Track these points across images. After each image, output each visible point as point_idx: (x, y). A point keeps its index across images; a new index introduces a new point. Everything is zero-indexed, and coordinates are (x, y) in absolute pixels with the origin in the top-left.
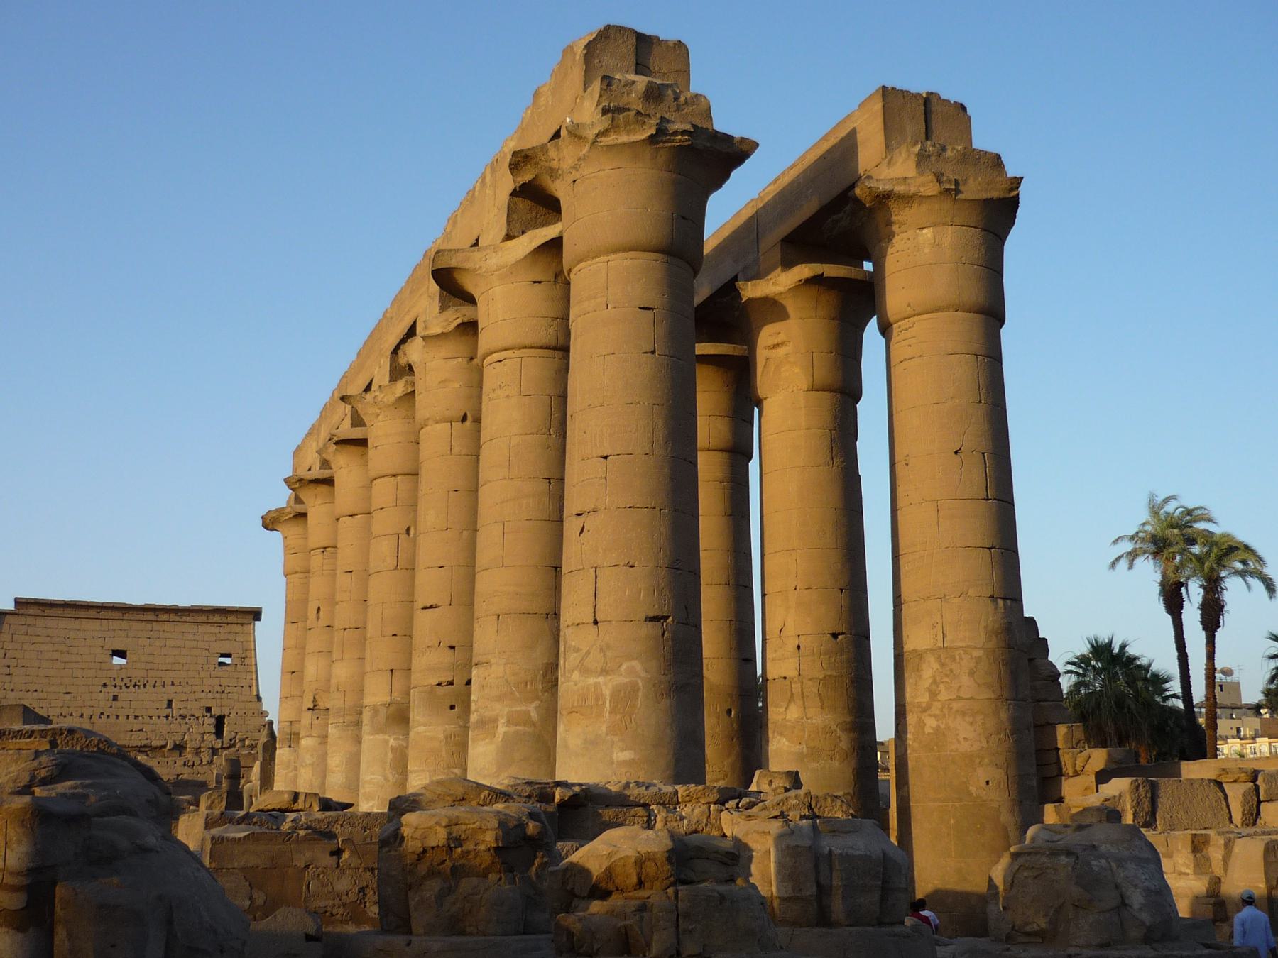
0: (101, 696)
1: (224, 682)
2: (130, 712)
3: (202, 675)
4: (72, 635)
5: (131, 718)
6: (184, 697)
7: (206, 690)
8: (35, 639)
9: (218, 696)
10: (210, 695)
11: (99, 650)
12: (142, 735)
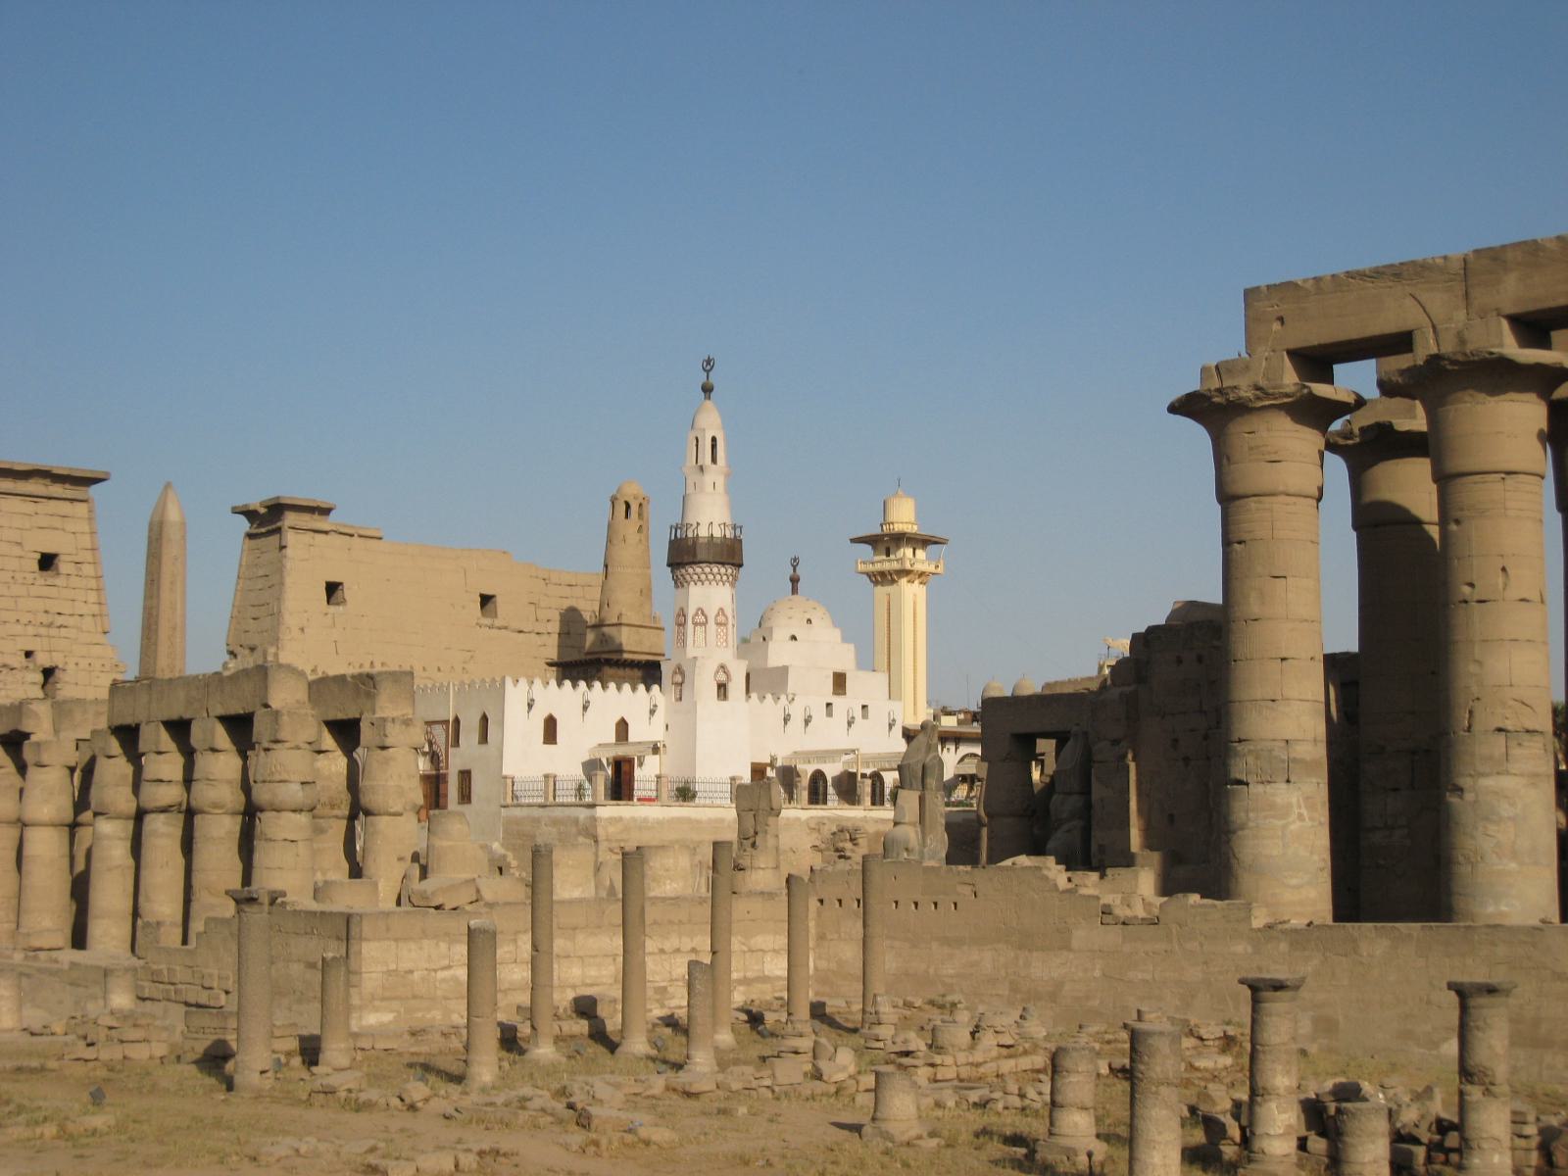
7: (24, 620)
9: (43, 631)
10: (31, 630)
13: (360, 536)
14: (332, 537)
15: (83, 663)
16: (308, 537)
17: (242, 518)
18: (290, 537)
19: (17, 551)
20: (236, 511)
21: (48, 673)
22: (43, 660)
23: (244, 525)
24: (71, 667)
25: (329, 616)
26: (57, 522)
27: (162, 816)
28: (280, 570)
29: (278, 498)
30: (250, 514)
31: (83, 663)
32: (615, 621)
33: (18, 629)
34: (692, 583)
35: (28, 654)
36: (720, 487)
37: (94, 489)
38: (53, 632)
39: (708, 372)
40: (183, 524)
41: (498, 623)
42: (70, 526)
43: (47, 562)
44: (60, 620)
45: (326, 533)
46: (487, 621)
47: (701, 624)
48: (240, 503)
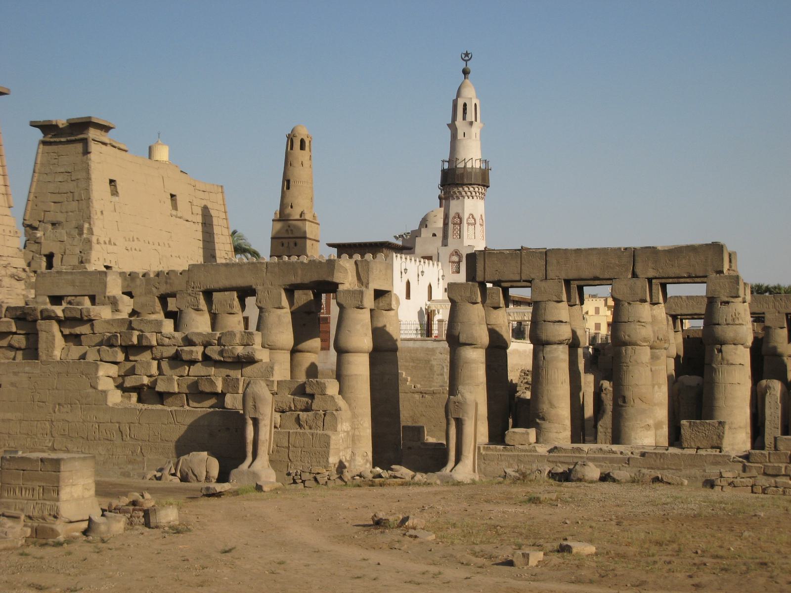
13: (120, 149)
14: (109, 148)
17: (38, 130)
18: (94, 147)
20: (34, 124)
23: (38, 134)
25: (113, 203)
28: (87, 170)
29: (90, 117)
30: (47, 128)
32: (298, 217)
34: (466, 197)
36: (478, 136)
39: (466, 61)
46: (174, 212)
47: (472, 224)
48: (42, 118)
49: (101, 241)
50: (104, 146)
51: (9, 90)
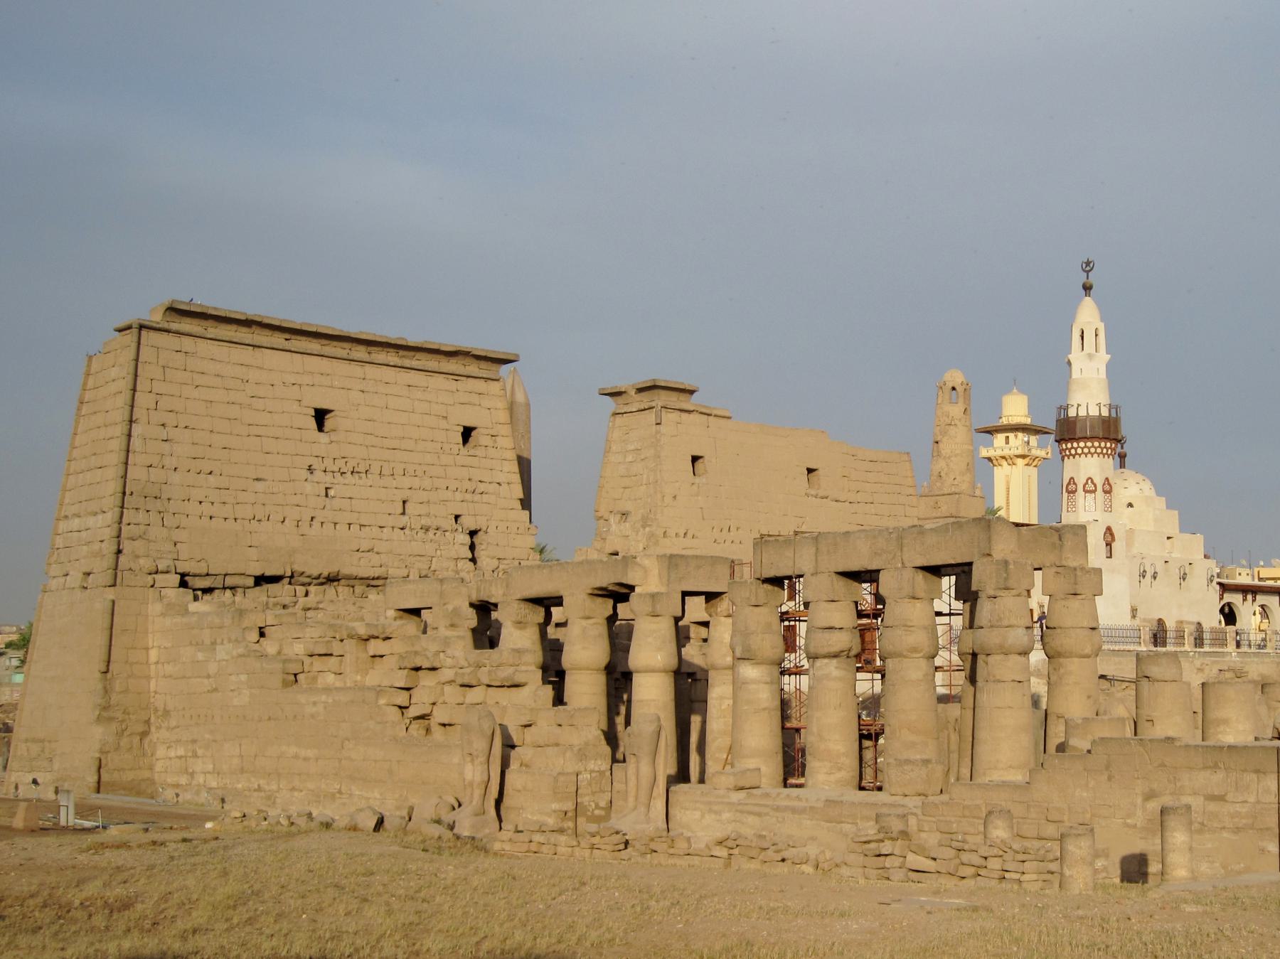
0: (308, 488)
1: (477, 474)
2: (352, 518)
3: (446, 459)
4: (253, 375)
5: (355, 528)
6: (424, 496)
7: (452, 487)
8: (199, 380)
9: (468, 496)
10: (458, 496)
11: (295, 407)
12: (376, 559)
15: (502, 527)
16: (674, 416)
19: (443, 424)
21: (473, 534)
22: (469, 522)
24: (491, 530)
26: (475, 399)
27: (834, 661)
31: (502, 527)
33: (449, 494)
35: (457, 517)
37: (505, 369)
38: (477, 497)
40: (528, 405)
41: (821, 493)
42: (486, 402)
43: (467, 433)
44: (482, 487)
45: (689, 412)
49: (671, 533)
50: (685, 415)
51: (517, 356)
